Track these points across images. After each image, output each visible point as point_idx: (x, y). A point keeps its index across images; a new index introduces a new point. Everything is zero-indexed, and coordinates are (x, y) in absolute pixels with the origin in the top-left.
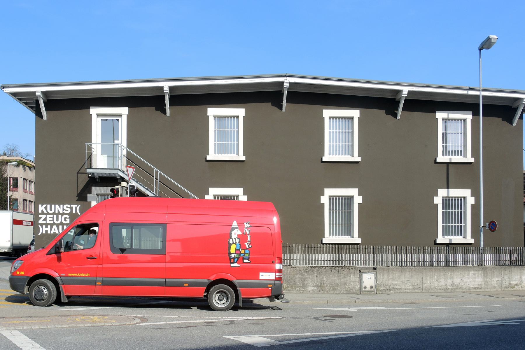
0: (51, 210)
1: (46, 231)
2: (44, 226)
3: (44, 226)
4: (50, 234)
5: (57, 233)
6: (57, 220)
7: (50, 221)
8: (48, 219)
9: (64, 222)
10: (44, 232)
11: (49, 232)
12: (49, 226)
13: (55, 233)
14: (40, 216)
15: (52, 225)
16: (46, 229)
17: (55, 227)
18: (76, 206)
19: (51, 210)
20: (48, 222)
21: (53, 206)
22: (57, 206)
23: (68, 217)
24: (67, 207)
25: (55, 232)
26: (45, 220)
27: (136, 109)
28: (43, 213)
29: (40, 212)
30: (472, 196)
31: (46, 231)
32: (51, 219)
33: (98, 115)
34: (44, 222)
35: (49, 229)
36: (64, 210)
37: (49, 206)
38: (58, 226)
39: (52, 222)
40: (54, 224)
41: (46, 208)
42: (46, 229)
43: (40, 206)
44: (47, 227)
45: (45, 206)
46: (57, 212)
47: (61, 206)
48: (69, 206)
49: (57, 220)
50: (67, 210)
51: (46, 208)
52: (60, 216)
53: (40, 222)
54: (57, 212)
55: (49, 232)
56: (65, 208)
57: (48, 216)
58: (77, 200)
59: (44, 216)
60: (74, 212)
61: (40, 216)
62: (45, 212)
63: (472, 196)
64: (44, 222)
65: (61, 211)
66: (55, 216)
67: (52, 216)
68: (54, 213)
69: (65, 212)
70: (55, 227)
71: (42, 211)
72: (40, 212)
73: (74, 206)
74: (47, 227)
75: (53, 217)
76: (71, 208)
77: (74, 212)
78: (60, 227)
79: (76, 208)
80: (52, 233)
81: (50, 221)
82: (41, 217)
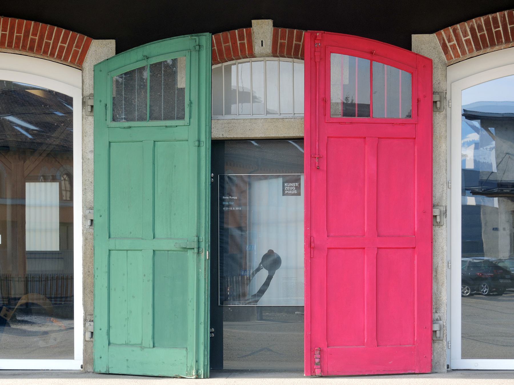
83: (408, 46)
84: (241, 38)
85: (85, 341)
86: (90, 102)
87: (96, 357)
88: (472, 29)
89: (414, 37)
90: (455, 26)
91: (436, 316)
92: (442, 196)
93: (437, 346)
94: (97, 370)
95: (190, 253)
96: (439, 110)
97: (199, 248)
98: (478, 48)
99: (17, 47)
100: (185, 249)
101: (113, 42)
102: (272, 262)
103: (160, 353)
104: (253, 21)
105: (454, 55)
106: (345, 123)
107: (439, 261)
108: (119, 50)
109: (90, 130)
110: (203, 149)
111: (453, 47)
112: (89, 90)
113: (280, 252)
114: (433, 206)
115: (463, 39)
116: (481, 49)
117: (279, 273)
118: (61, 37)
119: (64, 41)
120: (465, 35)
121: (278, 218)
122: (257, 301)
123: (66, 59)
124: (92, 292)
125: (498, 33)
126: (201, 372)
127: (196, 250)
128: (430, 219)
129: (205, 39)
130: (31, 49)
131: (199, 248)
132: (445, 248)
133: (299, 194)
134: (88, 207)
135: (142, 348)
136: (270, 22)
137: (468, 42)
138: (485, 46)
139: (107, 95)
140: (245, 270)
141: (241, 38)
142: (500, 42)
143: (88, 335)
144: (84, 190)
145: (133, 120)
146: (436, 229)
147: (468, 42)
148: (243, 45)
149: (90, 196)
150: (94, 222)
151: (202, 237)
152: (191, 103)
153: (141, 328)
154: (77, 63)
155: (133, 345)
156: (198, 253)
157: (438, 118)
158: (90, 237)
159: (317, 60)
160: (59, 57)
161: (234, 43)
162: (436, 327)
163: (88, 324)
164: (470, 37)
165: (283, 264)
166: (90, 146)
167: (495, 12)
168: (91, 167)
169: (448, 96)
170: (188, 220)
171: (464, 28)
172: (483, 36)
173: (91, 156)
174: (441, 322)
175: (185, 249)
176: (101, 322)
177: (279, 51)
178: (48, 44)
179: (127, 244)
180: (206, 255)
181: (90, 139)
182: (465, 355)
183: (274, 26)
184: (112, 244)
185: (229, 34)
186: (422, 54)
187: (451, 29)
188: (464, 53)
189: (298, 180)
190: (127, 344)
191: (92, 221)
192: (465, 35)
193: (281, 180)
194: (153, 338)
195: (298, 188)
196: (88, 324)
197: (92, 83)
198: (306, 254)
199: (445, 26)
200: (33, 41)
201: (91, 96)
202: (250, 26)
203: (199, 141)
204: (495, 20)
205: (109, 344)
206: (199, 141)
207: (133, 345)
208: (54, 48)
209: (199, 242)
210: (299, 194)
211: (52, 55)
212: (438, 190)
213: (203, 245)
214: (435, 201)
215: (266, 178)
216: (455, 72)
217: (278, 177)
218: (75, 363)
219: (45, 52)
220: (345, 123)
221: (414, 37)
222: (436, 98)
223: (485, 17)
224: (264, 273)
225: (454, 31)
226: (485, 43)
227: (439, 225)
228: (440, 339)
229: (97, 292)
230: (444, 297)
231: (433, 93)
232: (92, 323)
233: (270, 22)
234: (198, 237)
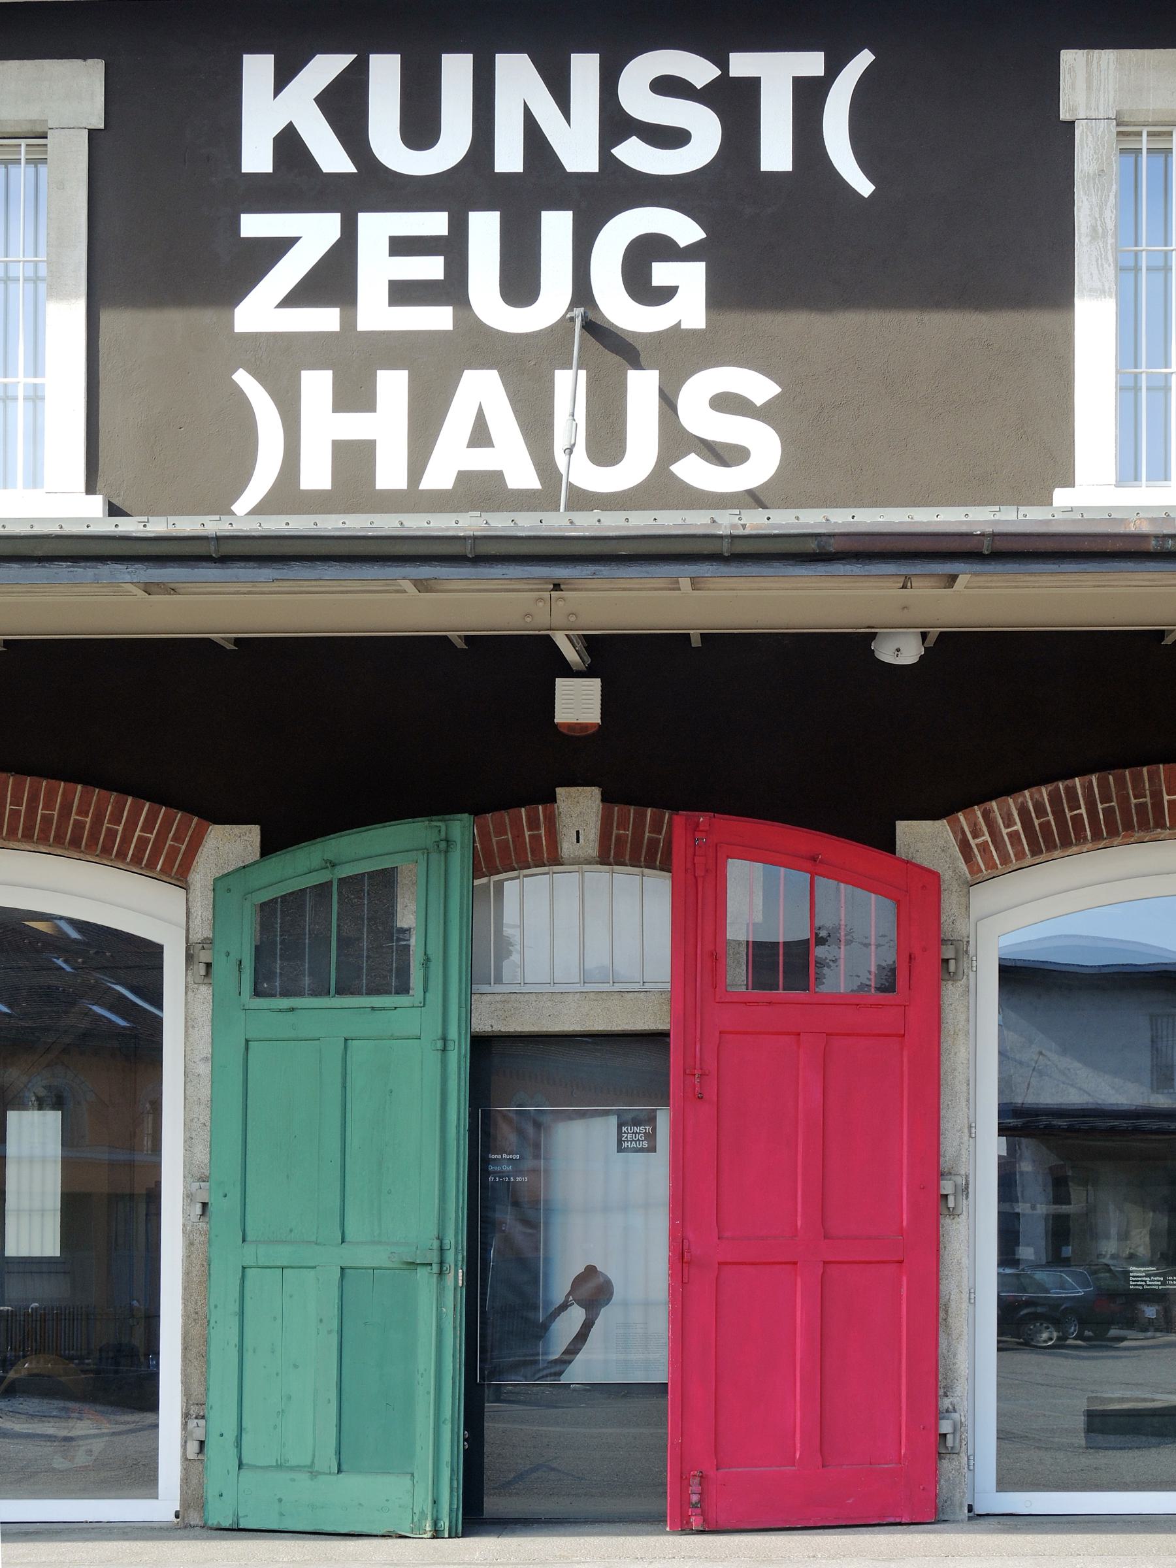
0: (420, 127)
1: (354, 458)
2: (316, 385)
3: (316, 385)
5: (522, 475)
6: (520, 282)
7: (403, 293)
8: (376, 269)
12: (393, 385)
13: (481, 489)
14: (256, 225)
15: (430, 374)
16: (354, 426)
17: (481, 390)
18: (812, 63)
19: (420, 127)
20: (375, 312)
21: (457, 71)
22: (517, 76)
23: (685, 230)
24: (667, 86)
25: (480, 460)
26: (333, 280)
28: (295, 179)
29: (257, 157)
31: (354, 458)
32: (431, 268)
35: (387, 422)
36: (616, 124)
37: (385, 74)
38: (526, 368)
40: (477, 345)
41: (345, 106)
42: (354, 426)
43: (258, 69)
44: (354, 395)
45: (325, 68)
46: (509, 157)
47: (585, 69)
48: (699, 71)
49: (520, 282)
50: (673, 138)
51: (345, 106)
52: (557, 228)
54: (509, 157)
55: (390, 474)
56: (637, 98)
57: (377, 228)
59: (315, 232)
60: (776, 153)
61: (256, 225)
62: (332, 156)
64: (323, 319)
65: (577, 148)
66: (485, 228)
67: (435, 223)
68: (468, 186)
69: (634, 154)
70: (481, 390)
71: (289, 143)
72: (257, 157)
73: (775, 72)
74: (354, 395)
75: (453, 248)
76: (736, 103)
77: (776, 153)
78: (569, 388)
79: (809, 97)
80: (439, 475)
81: (403, 293)
82: (280, 247)
83: (888, 844)
84: (534, 824)
85: (185, 1459)
86: (205, 956)
87: (211, 1493)
88: (1023, 812)
89: (902, 827)
90: (987, 805)
91: (945, 1403)
92: (959, 1155)
93: (947, 1466)
94: (213, 1522)
95: (422, 1272)
96: (953, 977)
97: (441, 1263)
98: (1036, 851)
99: (44, 839)
100: (412, 1265)
101: (256, 829)
102: (594, 1291)
103: (353, 1485)
104: (560, 791)
105: (984, 864)
106: (757, 1004)
107: (953, 1288)
108: (268, 848)
109: (203, 1012)
110: (453, 1056)
111: (983, 848)
112: (202, 930)
113: (611, 1270)
114: (941, 1175)
115: (1005, 831)
116: (1041, 852)
117: (607, 1317)
118: (142, 818)
119: (148, 827)
120: (1009, 823)
121: (612, 1204)
122: (560, 1373)
123: (151, 865)
124: (204, 1356)
125: (1077, 819)
126: (445, 1524)
127: (435, 1268)
128: (934, 1204)
129: (460, 827)
130: (75, 843)
131: (441, 1263)
132: (965, 1261)
133: (652, 1149)
134: (196, 1176)
135: (314, 1474)
136: (595, 792)
137: (1014, 836)
138: (1051, 846)
139: (242, 942)
140: (536, 1308)
141: (534, 824)
142: (1081, 838)
143: (193, 1447)
144: (189, 1142)
145: (299, 994)
146: (946, 1221)
147: (1014, 836)
148: (536, 839)
149: (201, 1154)
150: (211, 1208)
151: (450, 1240)
152: (428, 960)
153: (309, 1429)
154: (177, 873)
155: (292, 1468)
156: (441, 1273)
157: (951, 993)
158: (198, 1239)
159: (699, 873)
160: (137, 860)
161: (518, 836)
162: (945, 1427)
163: (192, 1424)
164: (1018, 827)
165: (616, 1297)
166: (204, 1048)
167: (1072, 777)
168: (205, 1092)
169: (971, 949)
170: (417, 1203)
171: (1007, 812)
172: (1045, 826)
173: (204, 1069)
174: (956, 1416)
175: (412, 1265)
176: (222, 1419)
177: (613, 852)
178: (111, 834)
179: (283, 1254)
180: (456, 1277)
181: (204, 1033)
182: (1004, 1484)
183: (603, 800)
184: (249, 1254)
185: (506, 816)
186: (918, 861)
187: (978, 811)
188: (1005, 859)
189: (651, 1120)
190: (279, 1467)
191: (205, 1205)
192: (1009, 823)
193: (613, 1121)
194: (339, 1452)
195: (651, 1137)
196: (192, 1424)
197: (209, 914)
198: (672, 1276)
199: (965, 804)
200: (79, 825)
201: (207, 943)
202: (553, 799)
203: (444, 1039)
204: (1071, 792)
205: (240, 1465)
206: (444, 1039)
207: (292, 1468)
208: (126, 840)
209: (442, 1250)
210: (652, 1149)
211: (121, 855)
212: (951, 1143)
213: (450, 1257)
214: (945, 1164)
215: (583, 1115)
216: (986, 897)
217: (606, 1113)
218: (164, 1505)
219: (106, 851)
220: (757, 1004)
221: (902, 827)
222: (948, 952)
223: (1051, 787)
224: (576, 1315)
225: (986, 815)
226: (1049, 840)
227: (953, 1213)
228: (953, 1452)
229: (213, 1356)
230: (962, 1364)
231: (944, 942)
232: (202, 1422)
233: (595, 792)
234: (440, 1239)
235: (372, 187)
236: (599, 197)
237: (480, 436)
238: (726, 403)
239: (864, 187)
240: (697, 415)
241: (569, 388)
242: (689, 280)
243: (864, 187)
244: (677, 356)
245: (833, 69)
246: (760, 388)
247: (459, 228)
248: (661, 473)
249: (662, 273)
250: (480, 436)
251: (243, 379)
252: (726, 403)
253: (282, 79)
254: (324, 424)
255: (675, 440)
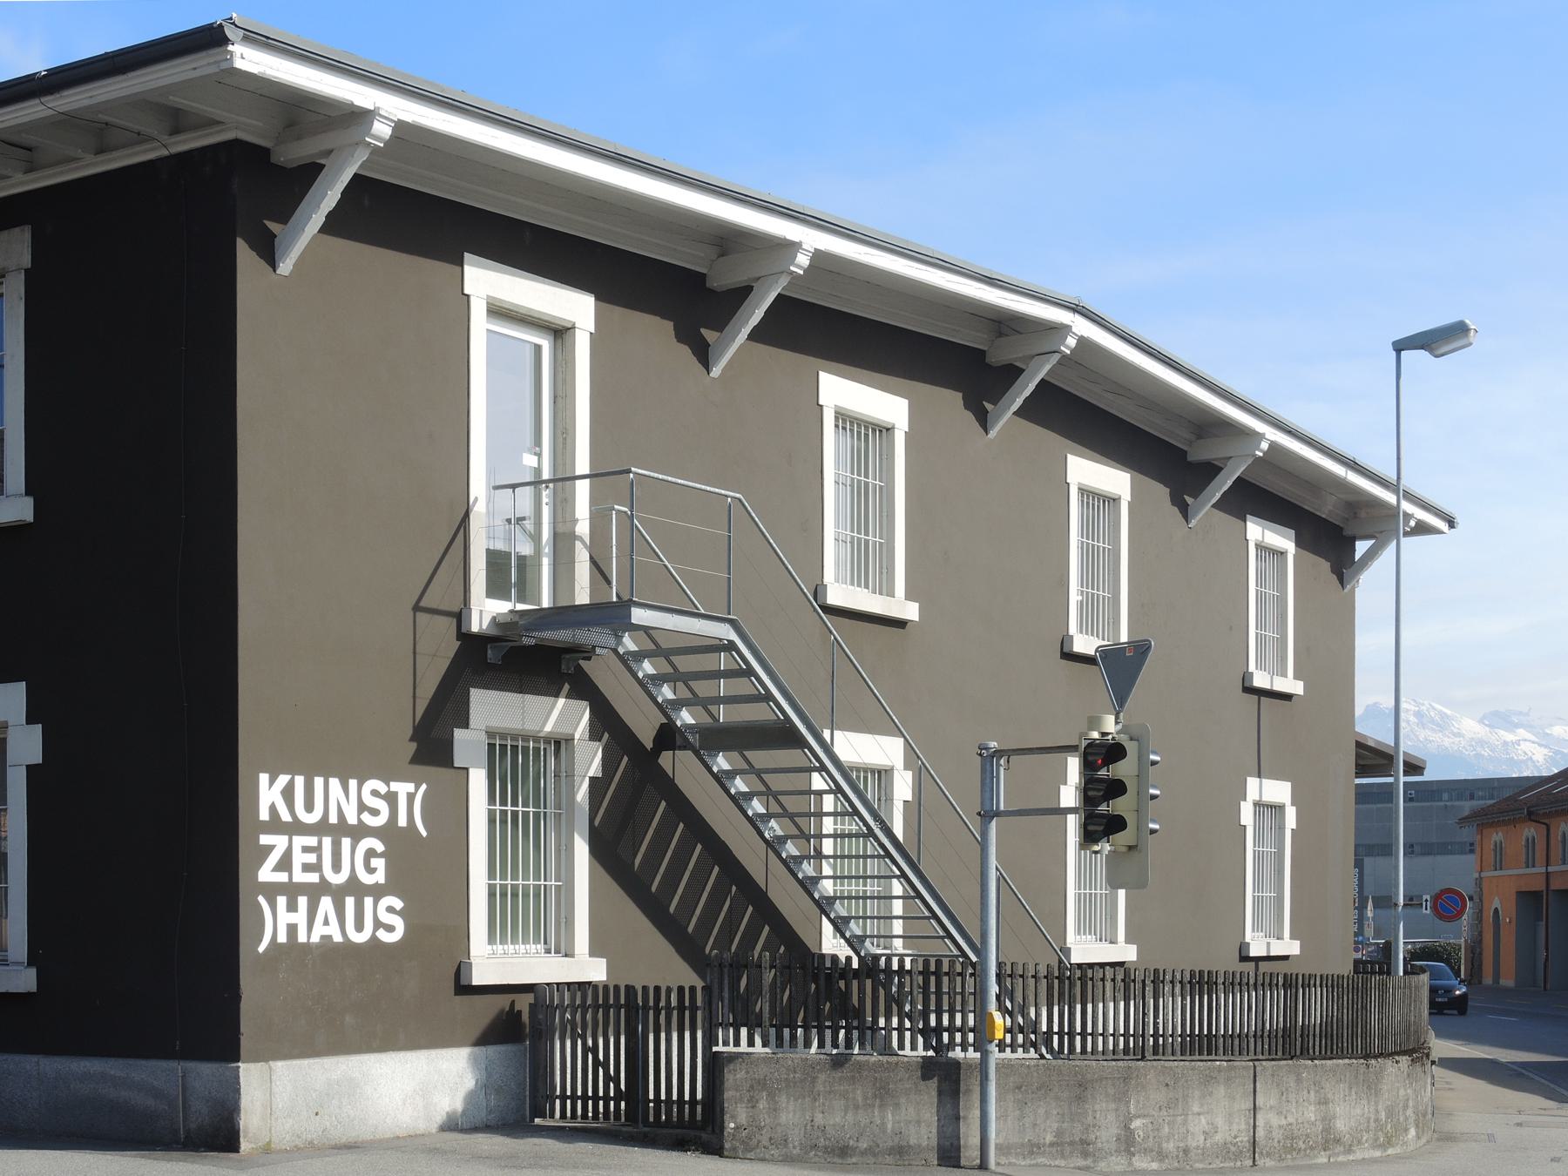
1: (292, 929)
2: (282, 901)
3: (282, 901)
4: (307, 947)
5: (338, 938)
7: (307, 868)
8: (299, 858)
9: (366, 879)
10: (282, 938)
11: (302, 938)
12: (303, 901)
14: (265, 839)
17: (326, 904)
18: (410, 787)
20: (300, 877)
21: (319, 782)
22: (334, 783)
25: (326, 931)
27: (618, 311)
28: (275, 825)
29: (264, 815)
30: (30, 720)
31: (292, 929)
32: (311, 858)
33: (497, 311)
34: (282, 877)
35: (300, 918)
36: (362, 807)
37: (300, 781)
38: (338, 894)
39: (313, 878)
41: (288, 793)
42: (292, 918)
43: (264, 778)
44: (292, 907)
45: (283, 780)
46: (333, 819)
47: (353, 783)
48: (382, 788)
51: (288, 793)
52: (346, 842)
53: (266, 874)
54: (333, 819)
55: (302, 938)
57: (300, 841)
58: (419, 758)
59: (279, 842)
60: (402, 821)
61: (265, 839)
62: (286, 817)
63: (30, 720)
66: (327, 842)
67: (312, 841)
68: (321, 828)
69: (368, 819)
70: (326, 904)
71: (273, 809)
72: (264, 815)
73: (402, 788)
74: (292, 907)
75: (317, 850)
76: (391, 798)
78: (350, 902)
80: (315, 939)
81: (307, 868)
82: (270, 848)
235: (297, 828)
236: (359, 832)
237: (326, 923)
238: (390, 909)
239: (424, 834)
240: (385, 917)
241: (350, 902)
242: (379, 863)
243: (424, 834)
244: (377, 892)
245: (417, 789)
246: (398, 904)
247: (320, 843)
248: (374, 938)
249: (375, 862)
250: (326, 923)
251: (261, 899)
252: (390, 909)
253: (272, 782)
254: (285, 918)
255: (378, 924)
